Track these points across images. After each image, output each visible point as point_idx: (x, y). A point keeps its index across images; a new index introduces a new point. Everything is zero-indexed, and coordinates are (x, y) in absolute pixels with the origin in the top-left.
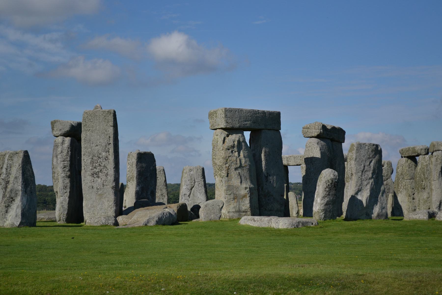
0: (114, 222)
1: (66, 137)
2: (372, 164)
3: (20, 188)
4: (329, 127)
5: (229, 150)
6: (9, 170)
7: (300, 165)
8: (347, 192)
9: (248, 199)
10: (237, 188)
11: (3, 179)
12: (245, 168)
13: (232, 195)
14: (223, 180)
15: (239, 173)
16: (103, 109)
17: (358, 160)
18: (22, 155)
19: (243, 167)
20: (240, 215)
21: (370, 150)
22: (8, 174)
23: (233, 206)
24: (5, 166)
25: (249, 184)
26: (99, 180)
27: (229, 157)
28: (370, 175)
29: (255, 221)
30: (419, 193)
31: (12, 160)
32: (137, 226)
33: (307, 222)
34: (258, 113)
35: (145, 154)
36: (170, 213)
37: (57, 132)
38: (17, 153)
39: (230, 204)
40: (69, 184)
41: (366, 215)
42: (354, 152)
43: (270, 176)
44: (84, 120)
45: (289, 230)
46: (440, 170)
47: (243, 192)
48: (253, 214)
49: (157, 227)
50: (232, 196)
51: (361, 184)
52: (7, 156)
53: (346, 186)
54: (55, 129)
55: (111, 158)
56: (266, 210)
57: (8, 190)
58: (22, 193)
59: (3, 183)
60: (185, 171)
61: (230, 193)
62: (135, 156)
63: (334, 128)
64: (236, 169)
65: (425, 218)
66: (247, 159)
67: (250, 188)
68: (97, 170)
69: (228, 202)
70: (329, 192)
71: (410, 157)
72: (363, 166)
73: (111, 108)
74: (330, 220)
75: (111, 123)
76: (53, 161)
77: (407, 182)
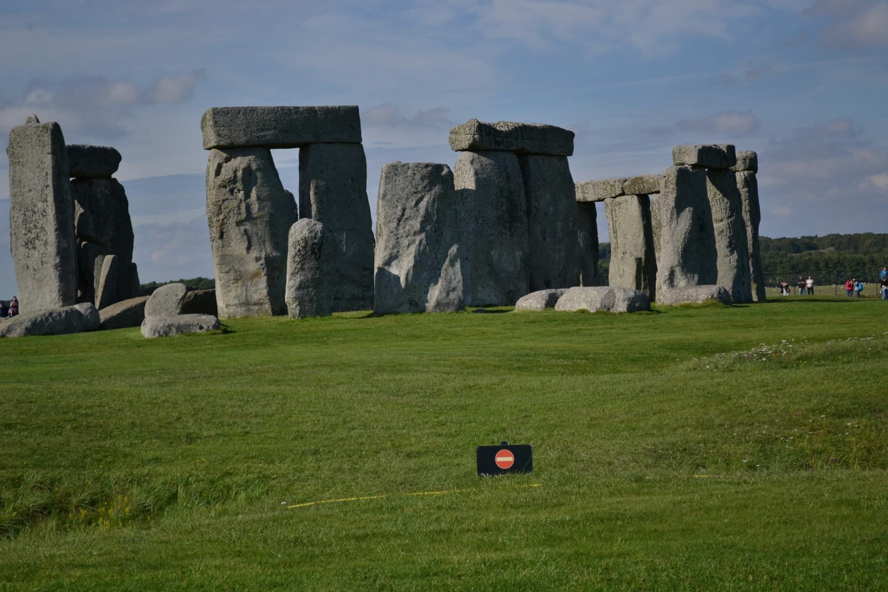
2: (423, 204)
5: (225, 187)
7: (603, 200)
10: (241, 260)
12: (258, 221)
13: (232, 273)
15: (245, 231)
17: (388, 197)
19: (256, 218)
20: (249, 310)
21: (418, 177)
27: (223, 201)
28: (417, 226)
33: (189, 325)
39: (230, 291)
41: (411, 304)
46: (673, 204)
47: (253, 267)
49: (27, 338)
50: (232, 275)
51: (397, 244)
61: (227, 269)
64: (239, 223)
65: (539, 306)
67: (266, 258)
68: (32, 236)
72: (399, 208)
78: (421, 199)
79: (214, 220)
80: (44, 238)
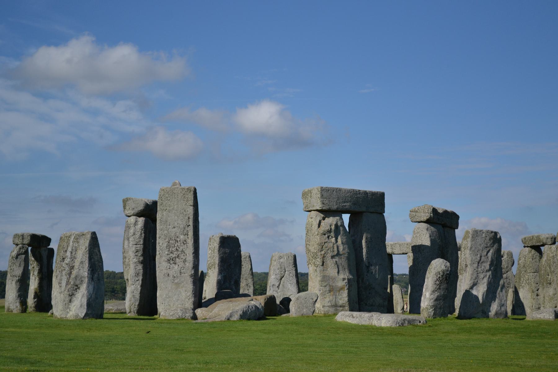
0: (192, 315)
1: (140, 217)
2: (490, 254)
3: (86, 274)
4: (440, 211)
5: (325, 235)
6: (74, 253)
7: (406, 254)
8: (460, 285)
9: (346, 292)
10: (334, 279)
11: (67, 264)
12: (342, 256)
13: (328, 287)
14: (318, 269)
15: (336, 262)
16: (183, 186)
17: (473, 249)
18: (89, 236)
19: (341, 255)
20: (337, 310)
21: (488, 238)
22: (73, 258)
24: (70, 249)
25: (348, 274)
26: (176, 267)
27: (325, 243)
28: (488, 267)
29: (353, 317)
30: (544, 288)
31: (78, 242)
32: (218, 320)
33: (414, 320)
34: (359, 193)
35: (229, 238)
36: (256, 307)
37: (129, 212)
39: (325, 298)
40: (142, 271)
42: (469, 240)
43: (371, 265)
44: (160, 197)
45: (393, 328)
48: (352, 310)
49: (241, 322)
50: (328, 288)
51: (477, 277)
52: (73, 237)
53: (459, 279)
54: (127, 208)
55: (190, 242)
56: (366, 304)
57: (73, 276)
58: (89, 280)
59: (67, 269)
61: (325, 284)
62: (218, 240)
63: (446, 212)
64: (333, 257)
65: (551, 318)
66: (346, 246)
68: (174, 256)
69: (323, 294)
70: (440, 285)
71: (533, 247)
72: (479, 256)
73: (192, 185)
74: (440, 317)
75: (191, 202)
76: (124, 244)
77: (529, 276)
79: (319, 254)
80: (184, 258)
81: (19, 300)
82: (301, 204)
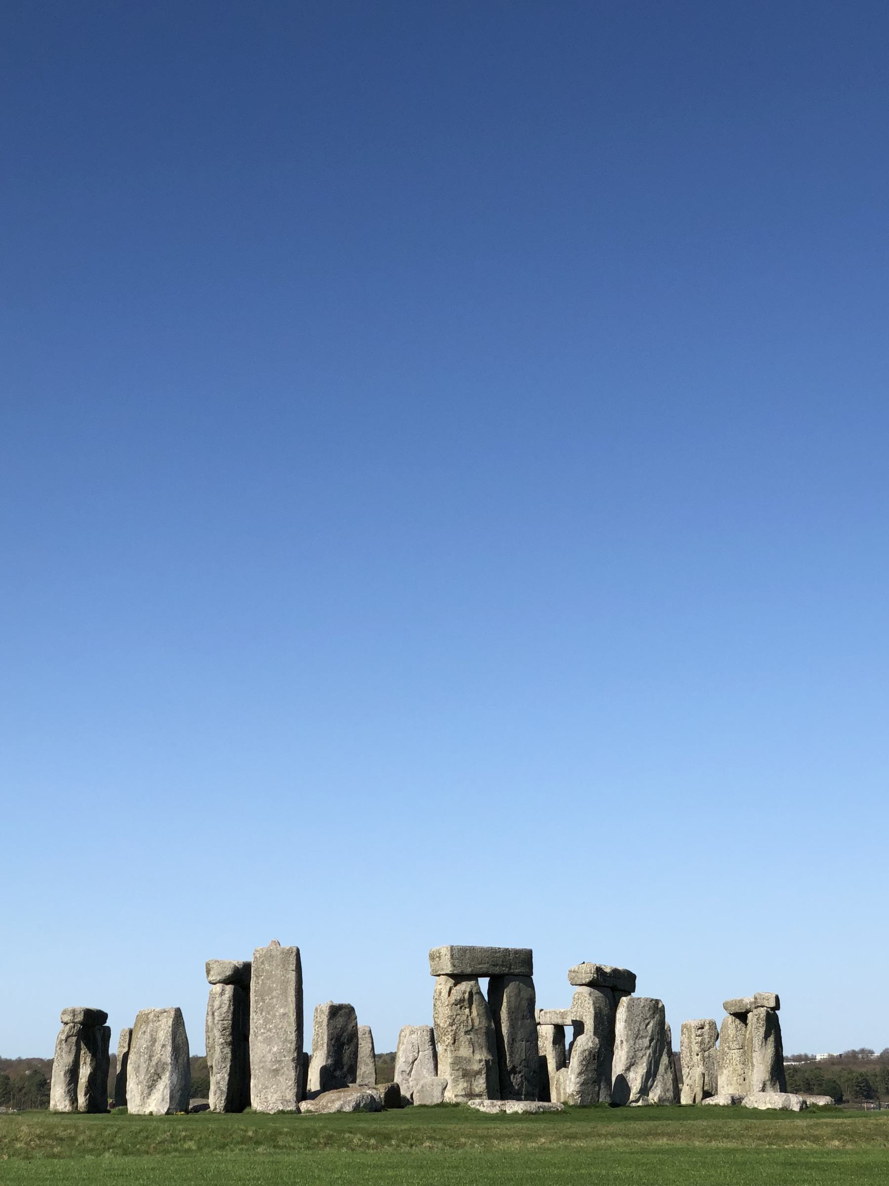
1: (227, 984)
4: (608, 970)
9: (484, 1076)
16: (282, 946)
18: (173, 1013)
23: (462, 1085)
36: (372, 1097)
37: (214, 978)
38: (165, 1012)
40: (230, 1055)
52: (152, 1014)
54: (212, 972)
60: (403, 1034)
63: (615, 971)
64: (467, 1033)
69: (455, 1081)
70: (587, 1066)
77: (735, 1054)
78: (648, 1024)
81: (68, 1098)
82: (427, 967)
